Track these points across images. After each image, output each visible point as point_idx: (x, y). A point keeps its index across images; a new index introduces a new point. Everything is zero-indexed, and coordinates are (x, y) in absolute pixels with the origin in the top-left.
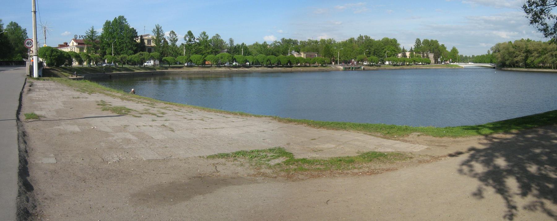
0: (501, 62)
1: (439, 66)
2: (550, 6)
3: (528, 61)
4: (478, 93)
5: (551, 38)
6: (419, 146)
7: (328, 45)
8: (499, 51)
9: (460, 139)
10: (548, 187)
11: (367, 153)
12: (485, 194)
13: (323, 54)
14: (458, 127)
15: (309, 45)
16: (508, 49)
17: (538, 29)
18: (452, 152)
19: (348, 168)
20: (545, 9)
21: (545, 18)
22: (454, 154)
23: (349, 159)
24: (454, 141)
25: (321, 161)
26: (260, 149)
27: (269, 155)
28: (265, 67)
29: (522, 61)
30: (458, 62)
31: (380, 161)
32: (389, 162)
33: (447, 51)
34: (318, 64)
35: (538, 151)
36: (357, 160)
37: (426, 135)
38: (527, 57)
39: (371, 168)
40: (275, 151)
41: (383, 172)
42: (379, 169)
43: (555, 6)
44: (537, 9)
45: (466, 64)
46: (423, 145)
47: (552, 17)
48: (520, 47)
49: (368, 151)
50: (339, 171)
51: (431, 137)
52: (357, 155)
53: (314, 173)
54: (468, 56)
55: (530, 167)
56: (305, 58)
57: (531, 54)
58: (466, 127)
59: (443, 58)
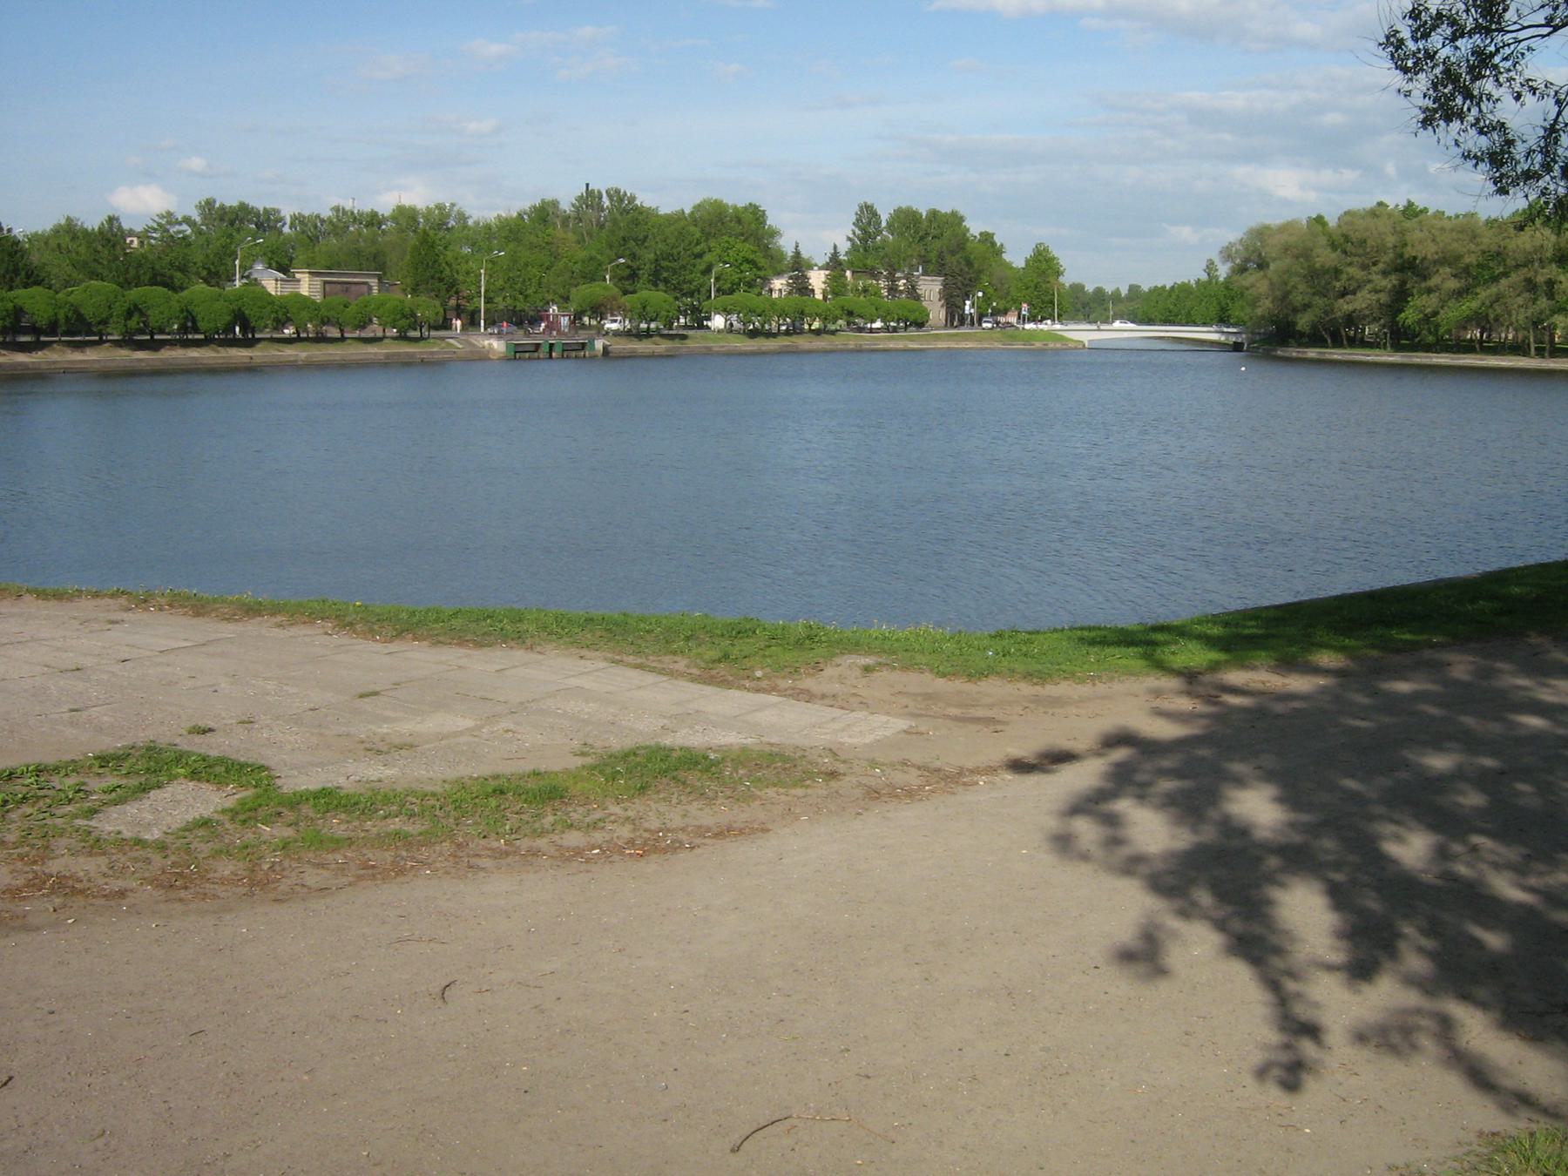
0: (1272, 319)
1: (966, 337)
2: (1522, 35)
3: (1409, 316)
4: (1154, 468)
5: (1526, 196)
6: (871, 717)
7: (431, 233)
8: (1262, 265)
9: (1063, 689)
10: (1478, 944)
11: (627, 755)
12: (1175, 957)
13: (409, 280)
14: (1055, 630)
15: (336, 235)
16: (1305, 254)
17: (1460, 151)
18: (1024, 749)
19: (537, 825)
20: (1497, 51)
21: (1496, 97)
22: (1033, 761)
23: (542, 783)
24: (1037, 700)
25: (409, 798)
26: (50, 760)
27: (95, 784)
28: (118, 344)
29: (1377, 314)
30: (1059, 316)
31: (688, 790)
32: (729, 793)
33: (1008, 266)
34: (384, 325)
35: (1439, 762)
36: (579, 786)
37: (905, 668)
38: (1401, 296)
39: (646, 825)
40: (127, 764)
41: (698, 841)
42: (683, 829)
43: (1548, 35)
44: (1458, 53)
45: (1099, 330)
46: (888, 714)
47: (1533, 90)
48: (1370, 242)
49: (629, 743)
50: (495, 844)
51: (928, 676)
52: (580, 761)
53: (374, 856)
54: (1109, 289)
55: (1399, 839)
56: (318, 298)
57: (1425, 278)
58: (1093, 634)
59: (987, 299)
